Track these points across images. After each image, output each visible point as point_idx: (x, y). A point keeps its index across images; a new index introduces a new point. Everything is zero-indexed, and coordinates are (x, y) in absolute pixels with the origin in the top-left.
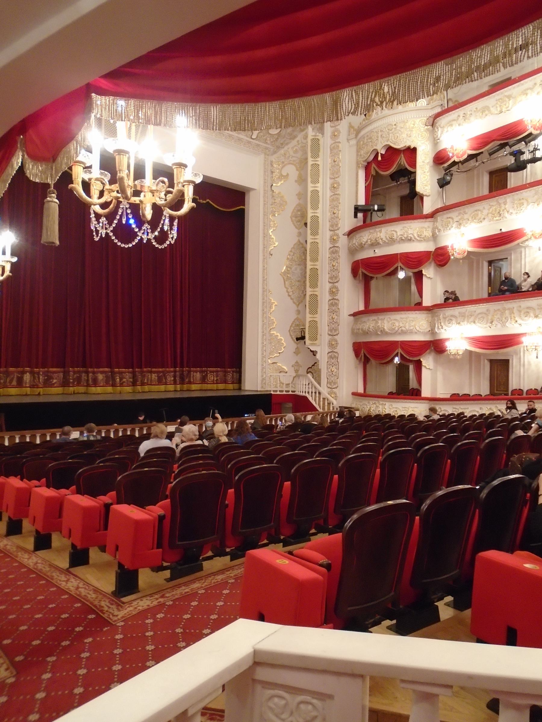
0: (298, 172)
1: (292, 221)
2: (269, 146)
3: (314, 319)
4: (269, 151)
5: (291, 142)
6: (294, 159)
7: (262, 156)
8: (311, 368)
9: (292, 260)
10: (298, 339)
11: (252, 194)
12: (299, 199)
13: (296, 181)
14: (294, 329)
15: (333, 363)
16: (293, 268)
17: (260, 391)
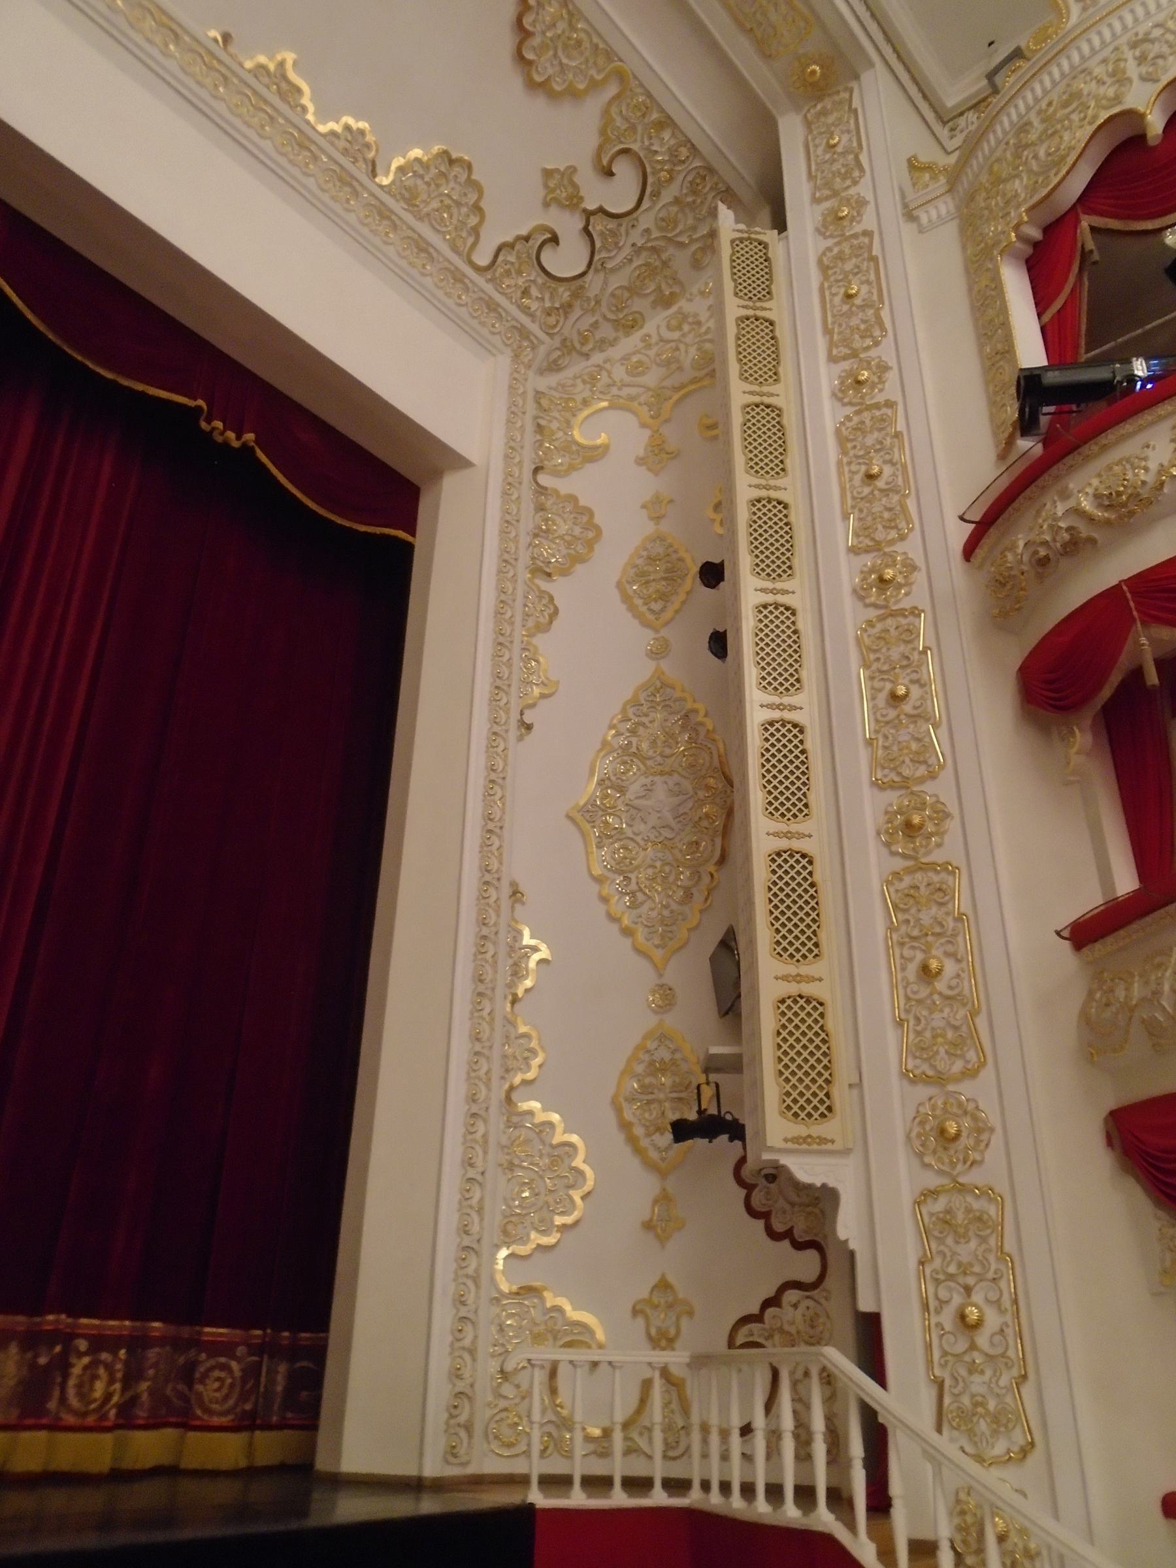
0: (647, 433)
1: (626, 598)
2: (534, 328)
3: (807, 989)
4: (534, 347)
5: (613, 343)
6: (633, 391)
7: (504, 361)
8: (757, 1318)
9: (628, 754)
10: (682, 1131)
11: (451, 484)
12: (657, 519)
13: (640, 461)
14: (646, 1089)
15: (964, 1269)
16: (634, 789)
17: (439, 1486)
